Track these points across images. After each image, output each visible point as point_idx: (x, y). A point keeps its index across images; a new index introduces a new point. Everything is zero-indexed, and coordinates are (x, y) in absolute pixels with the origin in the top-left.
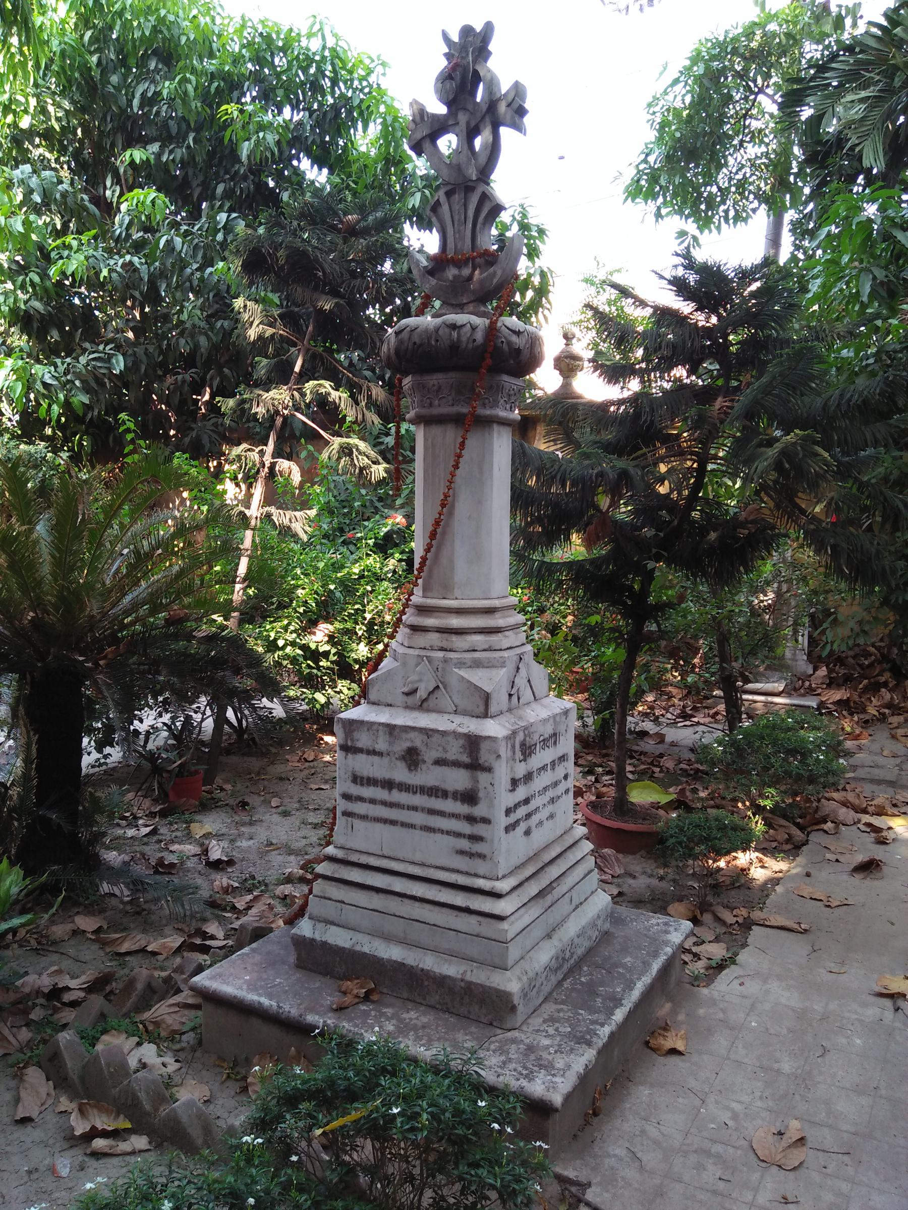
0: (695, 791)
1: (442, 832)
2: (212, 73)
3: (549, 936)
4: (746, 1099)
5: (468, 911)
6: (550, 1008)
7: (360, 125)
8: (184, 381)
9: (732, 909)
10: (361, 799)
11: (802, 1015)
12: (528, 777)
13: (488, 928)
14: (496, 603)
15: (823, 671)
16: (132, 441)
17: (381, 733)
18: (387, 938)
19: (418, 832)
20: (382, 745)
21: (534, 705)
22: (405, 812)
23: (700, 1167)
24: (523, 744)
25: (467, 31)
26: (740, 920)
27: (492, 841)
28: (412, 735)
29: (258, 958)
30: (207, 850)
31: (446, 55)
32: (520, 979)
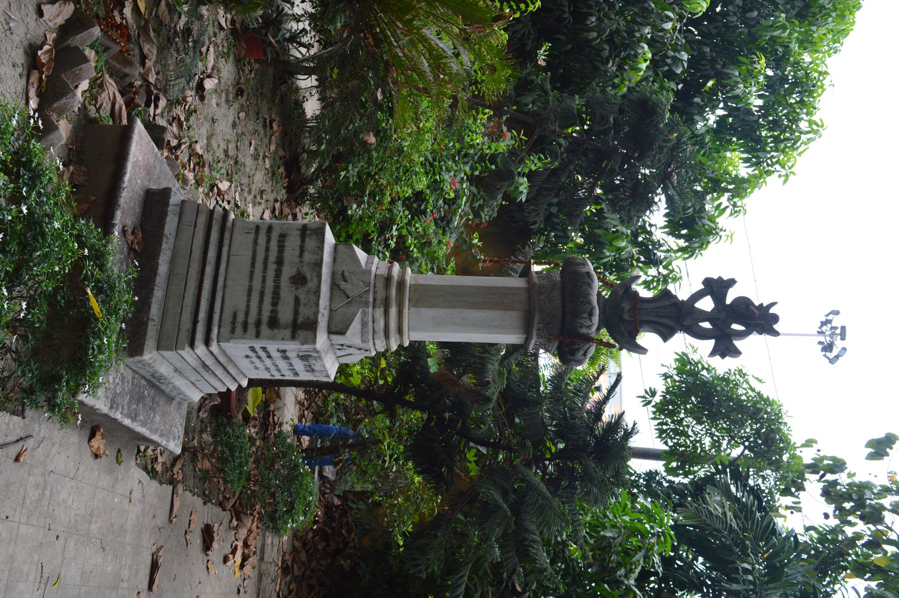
0: (254, 427)
1: (249, 301)
2: (788, 46)
3: (176, 370)
4: (75, 505)
5: (195, 322)
7: (745, 156)
8: (564, 12)
9: (181, 469)
10: (269, 240)
11: (122, 529)
12: (286, 358)
13: (184, 335)
15: (337, 502)
16: (519, 9)
17: (316, 256)
18: (172, 261)
19: (247, 283)
20: (307, 257)
21: (334, 357)
22: (261, 274)
23: (37, 486)
24: (309, 356)
25: (775, 319)
26: (175, 476)
27: (244, 338)
28: (315, 280)
29: (152, 161)
30: (209, 76)
31: (762, 304)
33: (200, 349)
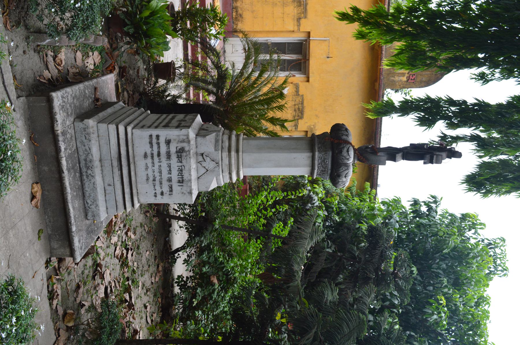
6: (75, 147)
14: (240, 153)
32: (93, 127)
33: (121, 128)
